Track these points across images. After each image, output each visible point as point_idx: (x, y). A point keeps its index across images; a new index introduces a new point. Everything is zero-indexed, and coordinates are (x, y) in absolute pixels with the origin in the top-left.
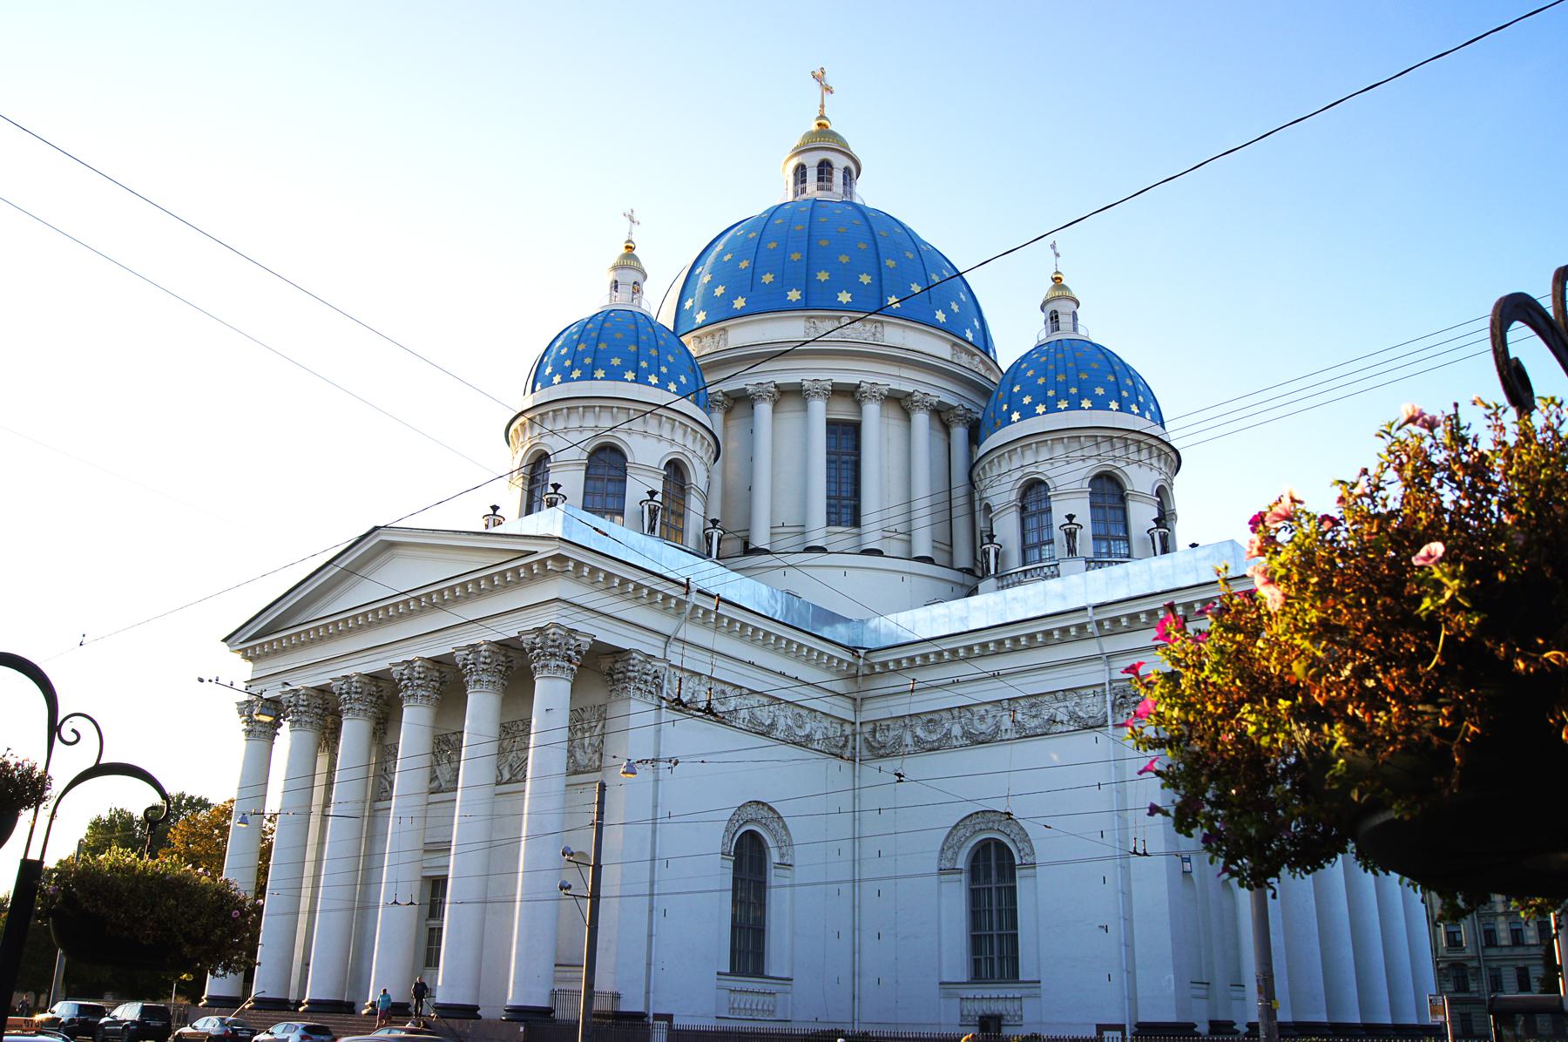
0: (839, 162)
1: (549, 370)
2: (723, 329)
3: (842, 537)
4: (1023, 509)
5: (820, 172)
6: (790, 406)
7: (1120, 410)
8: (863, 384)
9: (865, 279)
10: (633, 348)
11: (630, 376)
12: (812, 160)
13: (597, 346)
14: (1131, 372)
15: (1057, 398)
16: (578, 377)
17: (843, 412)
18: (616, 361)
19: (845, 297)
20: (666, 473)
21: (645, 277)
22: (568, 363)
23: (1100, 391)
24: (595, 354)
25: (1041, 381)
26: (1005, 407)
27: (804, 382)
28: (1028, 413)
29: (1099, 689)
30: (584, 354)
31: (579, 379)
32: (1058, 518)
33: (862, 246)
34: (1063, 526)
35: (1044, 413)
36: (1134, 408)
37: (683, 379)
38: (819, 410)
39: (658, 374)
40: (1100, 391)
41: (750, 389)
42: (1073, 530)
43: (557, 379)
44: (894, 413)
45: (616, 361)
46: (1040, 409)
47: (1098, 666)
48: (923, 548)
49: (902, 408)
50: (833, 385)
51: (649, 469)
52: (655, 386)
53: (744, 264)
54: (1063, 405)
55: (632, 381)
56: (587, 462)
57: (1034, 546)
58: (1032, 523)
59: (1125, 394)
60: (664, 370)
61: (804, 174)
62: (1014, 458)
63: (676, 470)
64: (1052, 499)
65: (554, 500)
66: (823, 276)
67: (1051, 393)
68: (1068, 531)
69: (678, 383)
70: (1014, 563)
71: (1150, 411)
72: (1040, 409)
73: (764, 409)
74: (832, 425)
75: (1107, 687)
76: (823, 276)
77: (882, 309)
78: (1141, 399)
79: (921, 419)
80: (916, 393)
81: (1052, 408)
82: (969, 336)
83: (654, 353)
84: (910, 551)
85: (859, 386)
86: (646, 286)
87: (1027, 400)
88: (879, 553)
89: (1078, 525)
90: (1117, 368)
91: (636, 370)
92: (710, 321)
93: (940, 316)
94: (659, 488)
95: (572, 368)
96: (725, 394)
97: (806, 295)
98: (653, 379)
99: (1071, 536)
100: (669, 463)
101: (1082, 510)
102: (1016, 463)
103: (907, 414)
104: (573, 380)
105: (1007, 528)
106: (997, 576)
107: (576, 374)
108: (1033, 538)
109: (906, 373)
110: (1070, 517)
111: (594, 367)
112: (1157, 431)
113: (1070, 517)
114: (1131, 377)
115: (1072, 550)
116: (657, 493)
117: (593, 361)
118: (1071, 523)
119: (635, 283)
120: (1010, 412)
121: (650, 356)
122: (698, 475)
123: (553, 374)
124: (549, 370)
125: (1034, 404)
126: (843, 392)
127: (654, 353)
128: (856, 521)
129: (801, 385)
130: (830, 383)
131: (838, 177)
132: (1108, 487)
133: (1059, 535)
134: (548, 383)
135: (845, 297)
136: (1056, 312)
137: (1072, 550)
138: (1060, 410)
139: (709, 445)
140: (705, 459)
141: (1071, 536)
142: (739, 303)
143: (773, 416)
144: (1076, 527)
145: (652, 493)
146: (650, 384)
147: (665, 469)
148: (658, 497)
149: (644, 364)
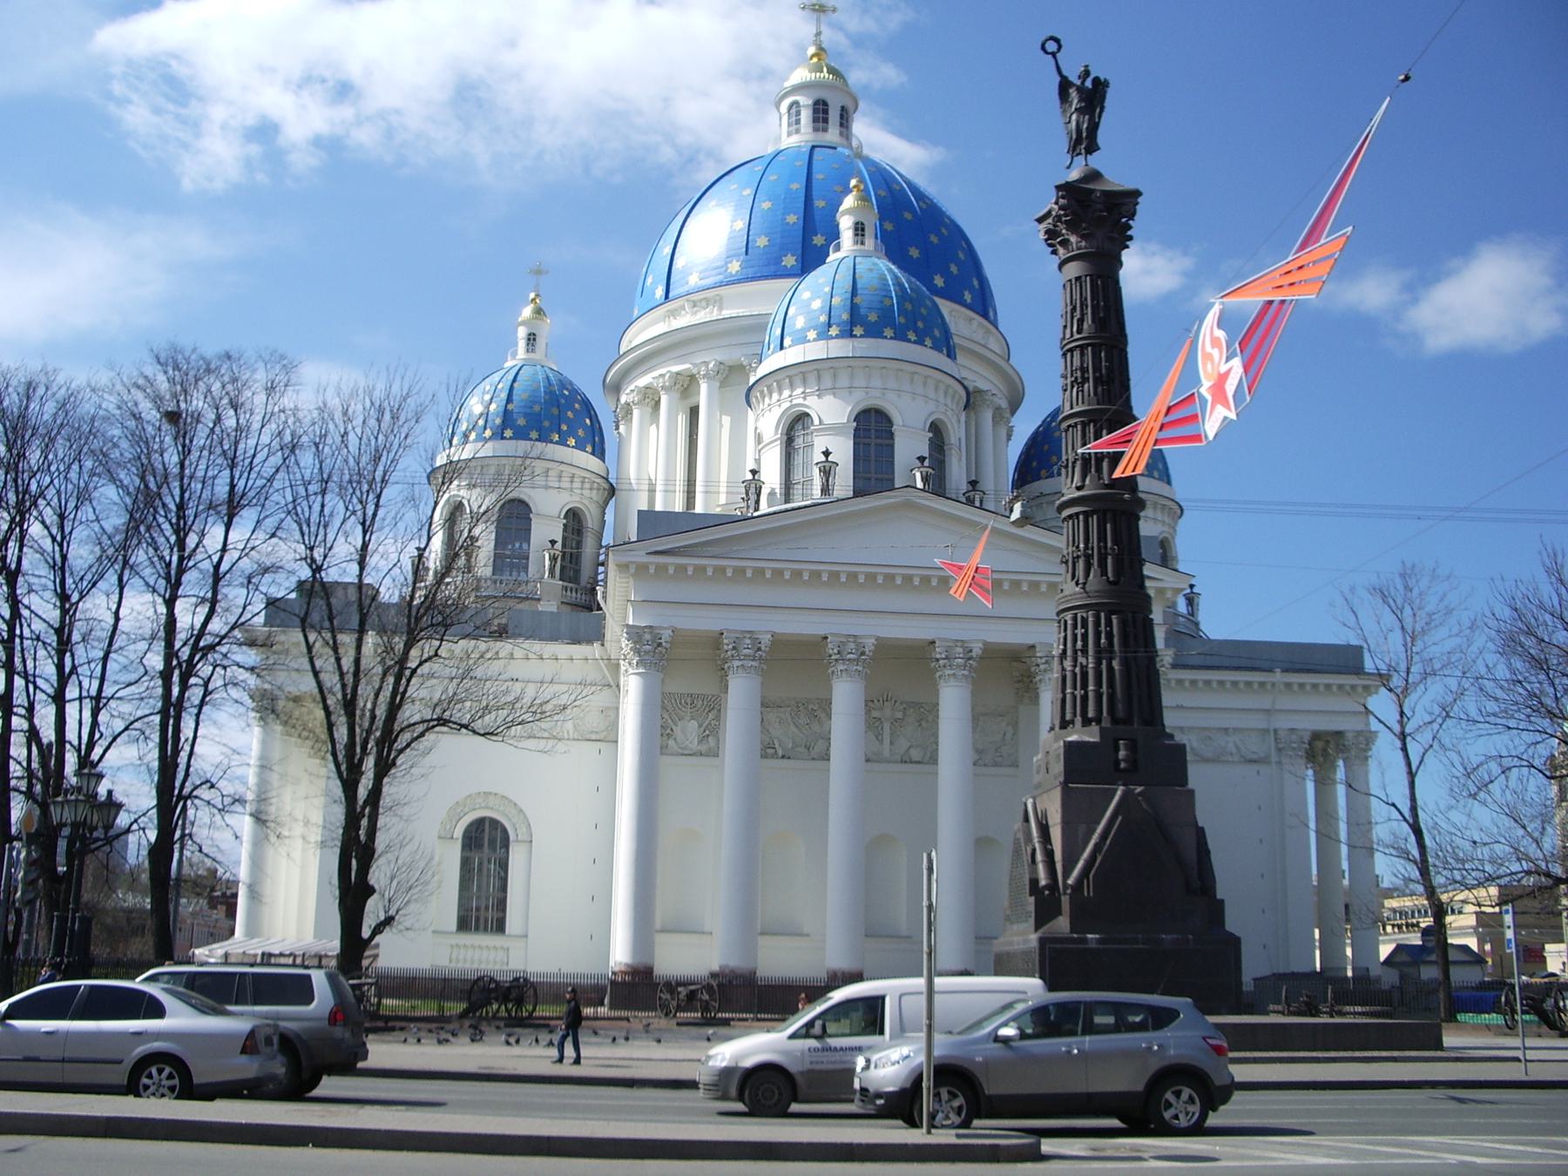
37: (937, 333)
39: (916, 331)
43: (812, 335)
52: (915, 342)
56: (855, 424)
60: (920, 324)
63: (937, 431)
65: (827, 469)
94: (926, 454)
98: (912, 336)
104: (832, 338)
107: (834, 331)
116: (925, 458)
122: (956, 433)
145: (922, 459)
146: (909, 341)
147: (929, 431)
148: (926, 463)
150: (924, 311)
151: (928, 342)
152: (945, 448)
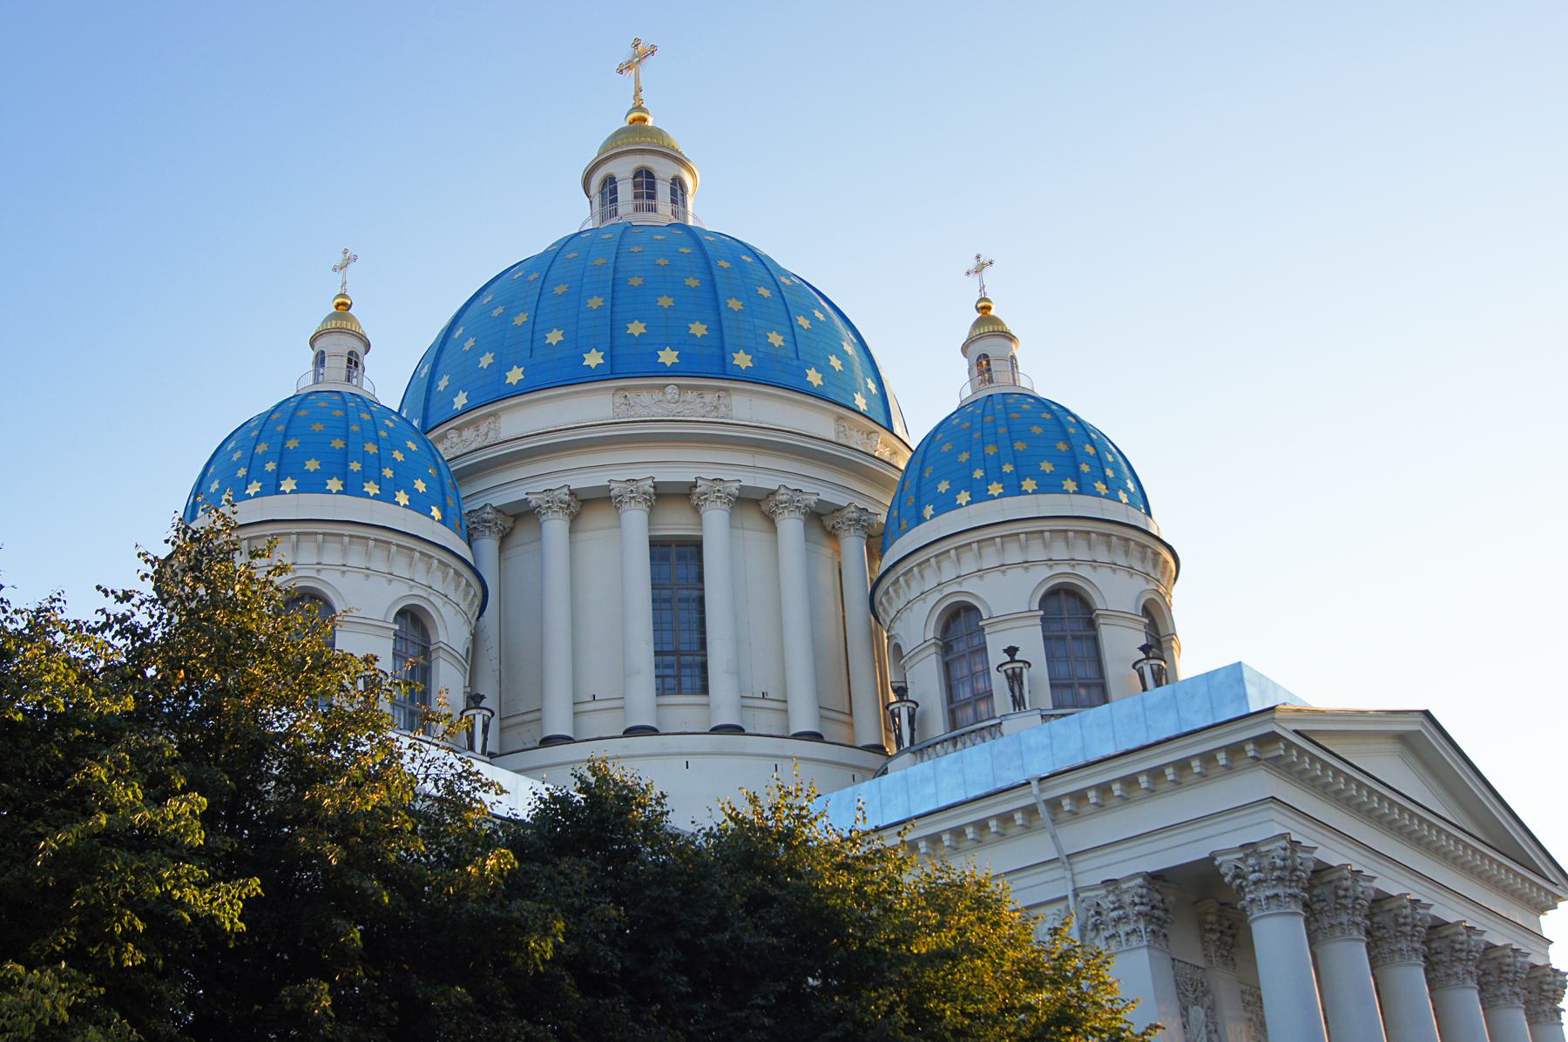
0: (663, 170)
1: (215, 486)
2: (490, 415)
3: (684, 710)
6: (596, 520)
7: (1080, 491)
8: (700, 482)
9: (698, 329)
10: (338, 444)
11: (334, 484)
12: (623, 169)
13: (284, 444)
14: (1093, 435)
15: (988, 480)
16: (256, 493)
17: (676, 524)
18: (312, 465)
19: (668, 357)
20: (397, 627)
21: (368, 347)
22: (242, 472)
23: (1047, 467)
24: (282, 456)
25: (964, 457)
27: (613, 485)
28: (946, 504)
29: (1061, 906)
30: (266, 457)
31: (257, 495)
32: (996, 656)
33: (692, 282)
34: (1001, 665)
35: (968, 503)
36: (1100, 487)
37: (420, 486)
38: (636, 524)
39: (379, 480)
40: (1047, 467)
41: (534, 501)
42: (1017, 670)
44: (751, 519)
45: (312, 465)
46: (963, 497)
47: (1055, 872)
48: (804, 720)
49: (763, 513)
50: (656, 486)
51: (365, 624)
52: (376, 497)
53: (520, 319)
54: (995, 489)
55: (338, 492)
57: (967, 703)
58: (961, 670)
59: (1085, 468)
60: (388, 473)
61: (614, 191)
62: (928, 573)
64: (987, 631)
66: (636, 328)
67: (978, 474)
68: (1010, 672)
69: (411, 492)
70: (937, 725)
71: (1126, 491)
72: (963, 497)
73: (555, 527)
74: (660, 548)
75: (1071, 898)
76: (636, 328)
77: (724, 372)
78: (1109, 473)
79: (791, 527)
80: (783, 490)
81: (979, 495)
82: (861, 402)
83: (371, 448)
84: (787, 728)
85: (694, 485)
86: (368, 360)
87: (943, 487)
88: (737, 730)
89: (1025, 662)
90: (1072, 431)
91: (344, 475)
92: (477, 402)
93: (814, 377)
95: (248, 481)
96: (498, 510)
97: (611, 357)
99: (1015, 679)
100: (402, 613)
101: (1032, 643)
102: (931, 580)
103: (770, 520)
105: (926, 680)
106: (913, 749)
107: (254, 488)
108: (964, 693)
109: (763, 460)
110: (1011, 651)
111: (279, 476)
112: (1137, 518)
114: (1092, 443)
115: (1018, 702)
117: (279, 465)
118: (1013, 661)
119: (351, 353)
121: (365, 454)
122: (451, 630)
123: (221, 491)
124: (215, 486)
125: (954, 492)
126: (664, 495)
127: (371, 448)
128: (704, 690)
129: (607, 489)
130: (650, 482)
131: (663, 191)
132: (1067, 604)
133: (999, 682)
135: (668, 357)
136: (985, 356)
137: (1018, 702)
138: (992, 498)
139: (468, 585)
140: (464, 606)
141: (1015, 679)
142: (515, 376)
143: (570, 537)
144: (1021, 665)
146: (367, 495)
147: (395, 621)
149: (355, 467)
150: (398, 456)
151: (402, 498)
152: (432, 648)
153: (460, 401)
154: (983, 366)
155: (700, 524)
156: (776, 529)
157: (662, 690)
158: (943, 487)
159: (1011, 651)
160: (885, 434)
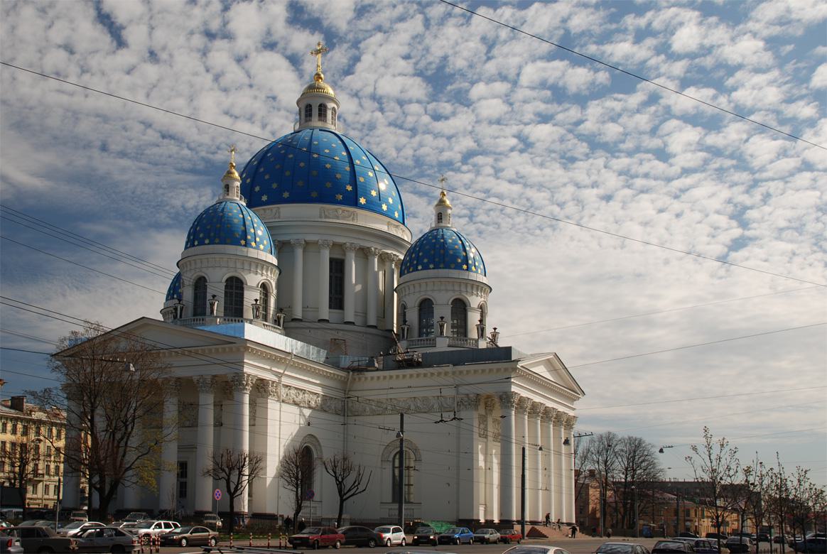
4: (420, 310)
5: (320, 110)
26: (415, 262)
32: (436, 319)
38: (326, 255)
61: (311, 110)
74: (332, 260)
87: (426, 261)
94: (258, 299)
113: (442, 318)
120: (417, 265)
134: (201, 243)
135: (340, 197)
136: (441, 213)
137: (442, 332)
142: (286, 195)
145: (256, 300)
148: (258, 303)
151: (262, 247)
153: (264, 198)
154: (440, 217)
155: (345, 255)
156: (368, 259)
157: (330, 307)
158: (426, 261)
159: (442, 318)
160: (402, 226)
